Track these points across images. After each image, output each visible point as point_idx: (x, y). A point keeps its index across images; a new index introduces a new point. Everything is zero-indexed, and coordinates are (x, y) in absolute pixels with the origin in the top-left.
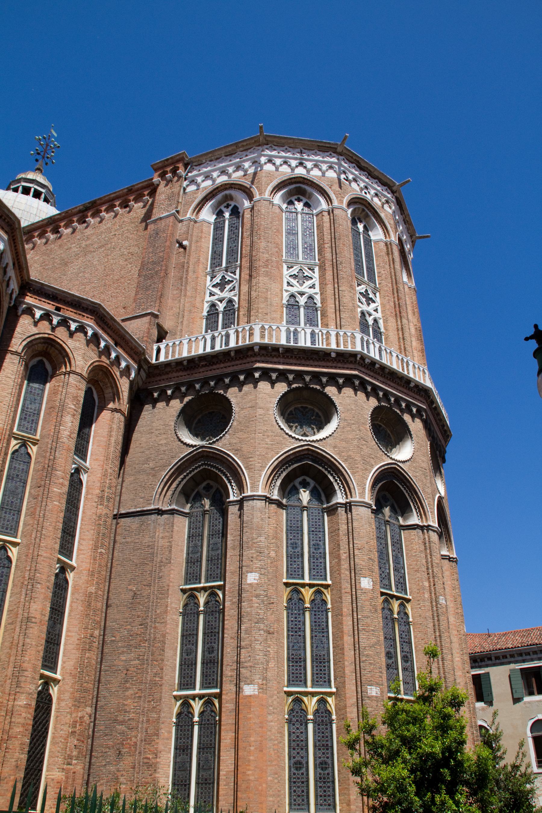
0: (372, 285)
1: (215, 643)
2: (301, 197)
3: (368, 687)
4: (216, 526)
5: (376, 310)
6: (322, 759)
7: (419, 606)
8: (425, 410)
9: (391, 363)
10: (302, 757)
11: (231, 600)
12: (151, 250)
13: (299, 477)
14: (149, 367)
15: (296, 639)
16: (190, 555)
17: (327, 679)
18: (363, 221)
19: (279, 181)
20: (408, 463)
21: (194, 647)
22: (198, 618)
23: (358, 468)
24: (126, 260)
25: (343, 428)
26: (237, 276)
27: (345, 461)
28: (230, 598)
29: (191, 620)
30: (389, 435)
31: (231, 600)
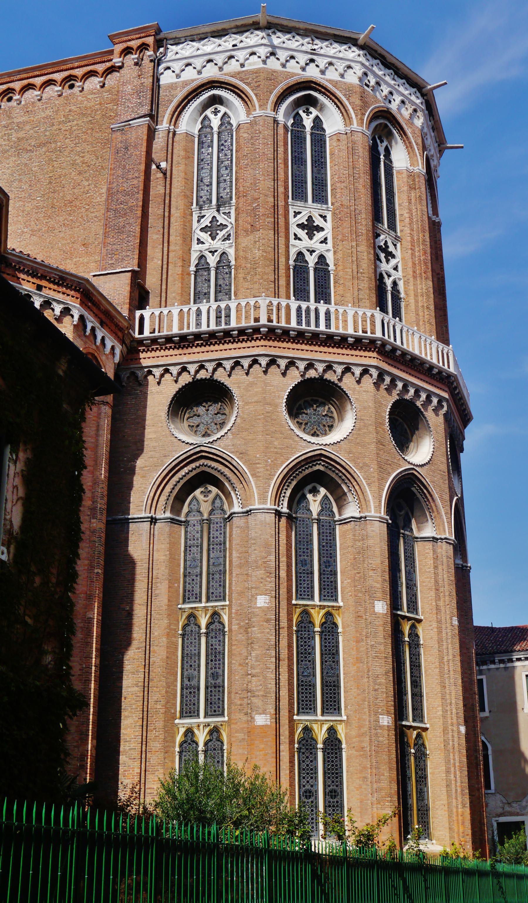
0: (392, 233)
1: (219, 668)
2: (312, 109)
3: (380, 716)
4: (217, 537)
5: (396, 269)
6: (331, 787)
7: (431, 628)
8: (447, 400)
9: (413, 349)
10: (312, 786)
11: (239, 624)
12: (120, 172)
13: (309, 484)
14: (131, 341)
15: (306, 665)
16: (188, 570)
17: (336, 707)
18: (385, 141)
19: (285, 88)
20: (426, 467)
21: (196, 673)
22: (200, 640)
23: (374, 477)
24: (80, 173)
25: (359, 429)
26: (233, 220)
27: (361, 469)
28: (237, 622)
29: (191, 643)
30: (406, 430)
31: (239, 624)
